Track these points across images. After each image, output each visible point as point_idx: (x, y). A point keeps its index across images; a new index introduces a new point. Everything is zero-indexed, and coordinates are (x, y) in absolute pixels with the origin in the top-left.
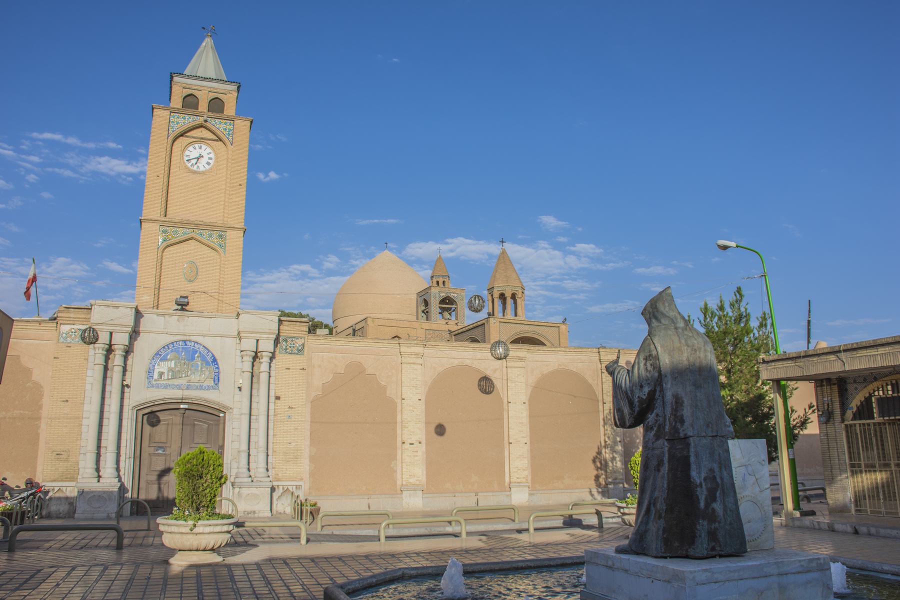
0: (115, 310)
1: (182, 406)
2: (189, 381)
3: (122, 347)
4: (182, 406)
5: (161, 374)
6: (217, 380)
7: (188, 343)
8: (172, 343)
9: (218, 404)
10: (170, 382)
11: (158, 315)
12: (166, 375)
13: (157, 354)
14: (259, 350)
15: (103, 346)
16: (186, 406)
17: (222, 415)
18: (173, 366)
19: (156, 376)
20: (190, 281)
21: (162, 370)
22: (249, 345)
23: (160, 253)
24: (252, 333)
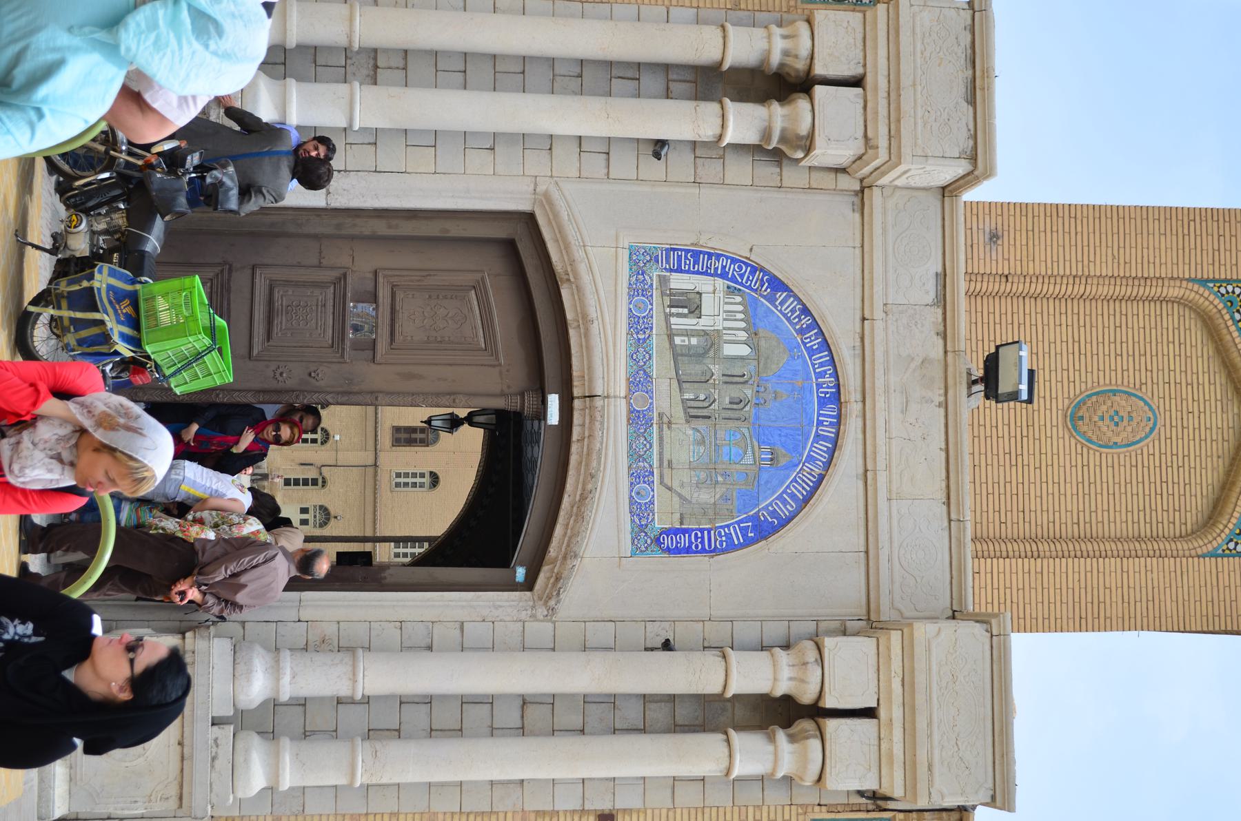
0: (960, 90)
1: (553, 401)
2: (666, 422)
3: (804, 129)
4: (553, 401)
5: (690, 304)
6: (679, 542)
7: (830, 410)
8: (826, 345)
9: (569, 554)
10: (657, 341)
11: (942, 278)
12: (689, 323)
13: (777, 284)
14: (831, 725)
15: (804, 51)
16: (553, 417)
17: (520, 573)
18: (729, 350)
19: (680, 282)
20: (1074, 418)
21: (708, 305)
22: (848, 673)
23: (1175, 292)
24: (908, 683)
